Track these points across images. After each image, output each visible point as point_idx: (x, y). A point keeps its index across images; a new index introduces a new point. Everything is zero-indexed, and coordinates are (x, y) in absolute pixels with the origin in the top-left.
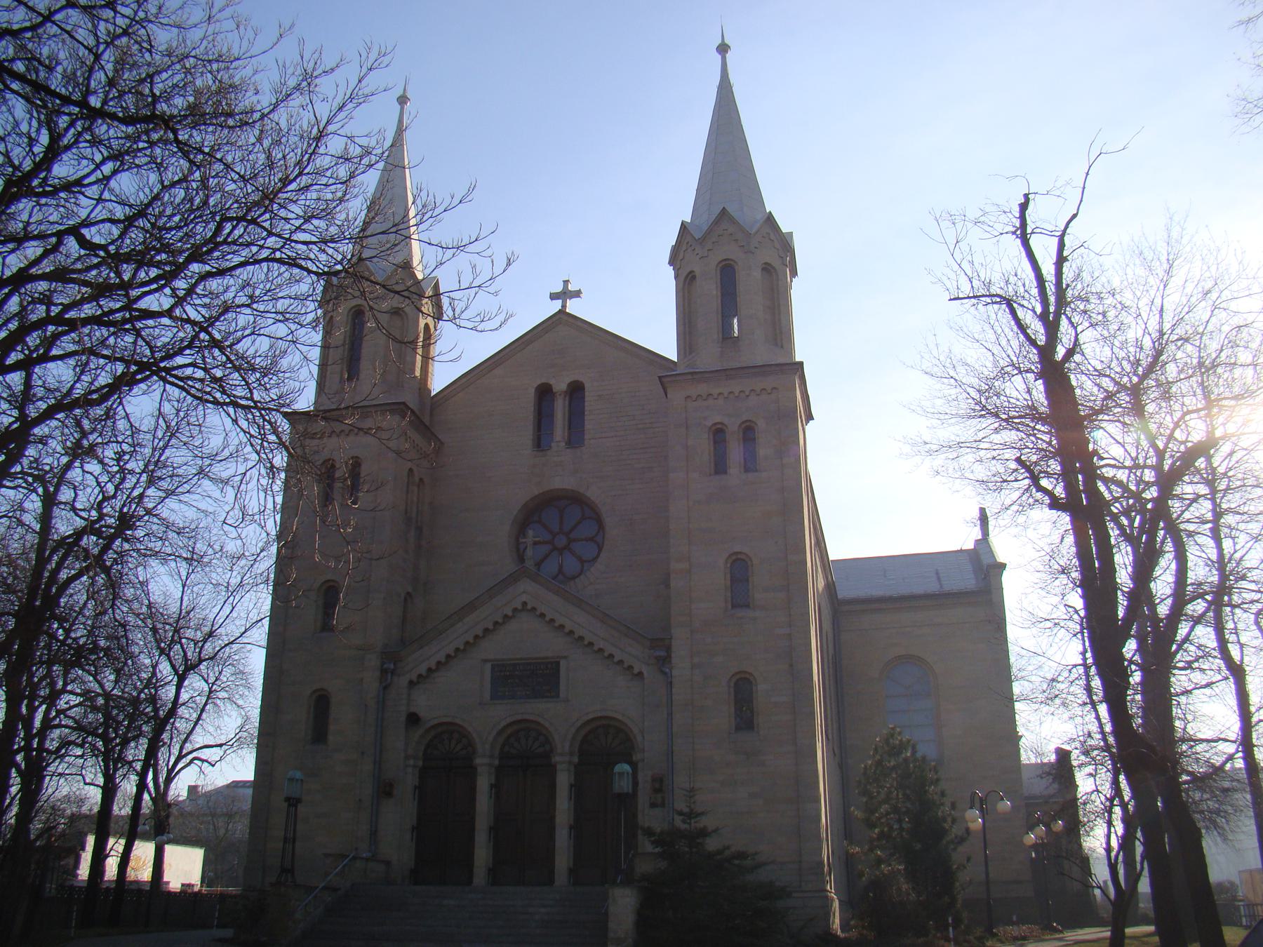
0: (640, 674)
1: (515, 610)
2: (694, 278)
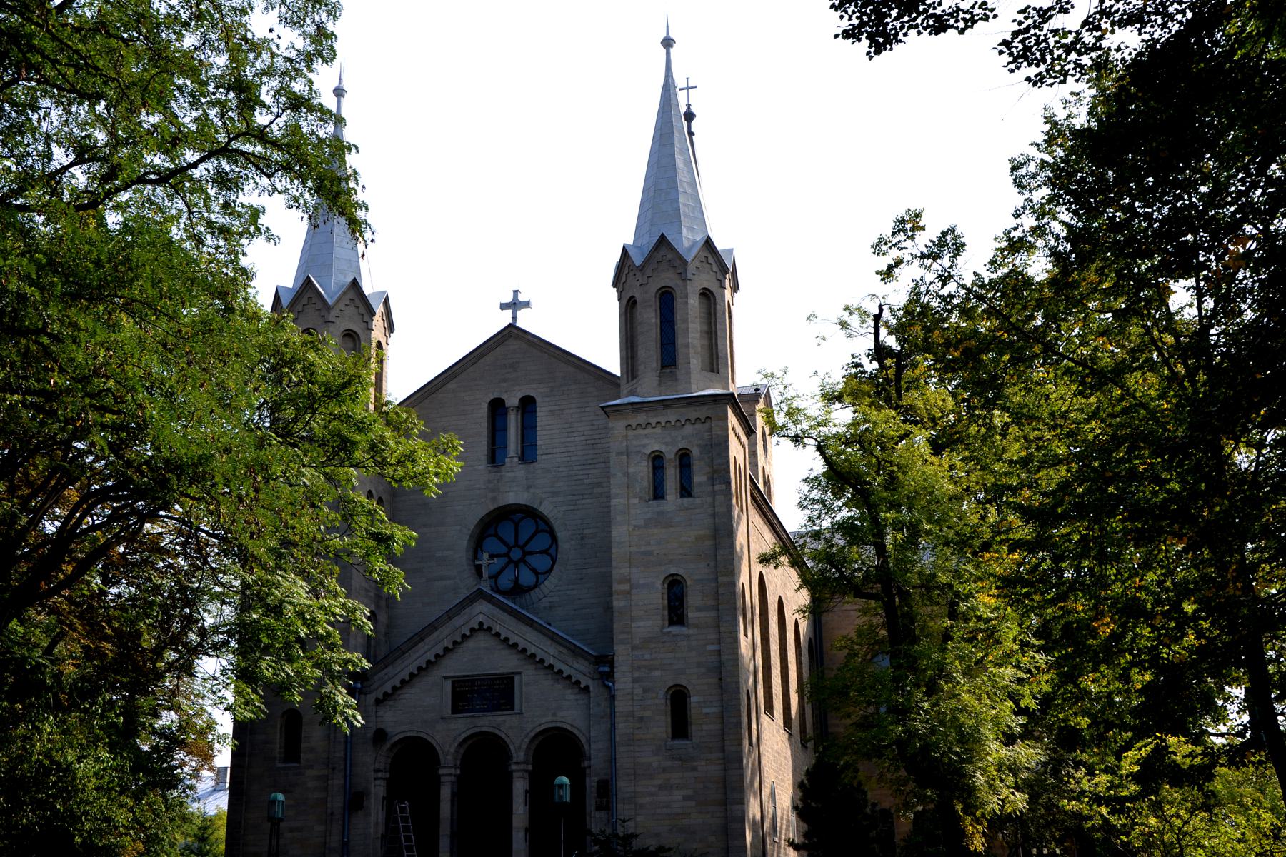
0: (587, 688)
1: (472, 630)
2: (635, 302)
